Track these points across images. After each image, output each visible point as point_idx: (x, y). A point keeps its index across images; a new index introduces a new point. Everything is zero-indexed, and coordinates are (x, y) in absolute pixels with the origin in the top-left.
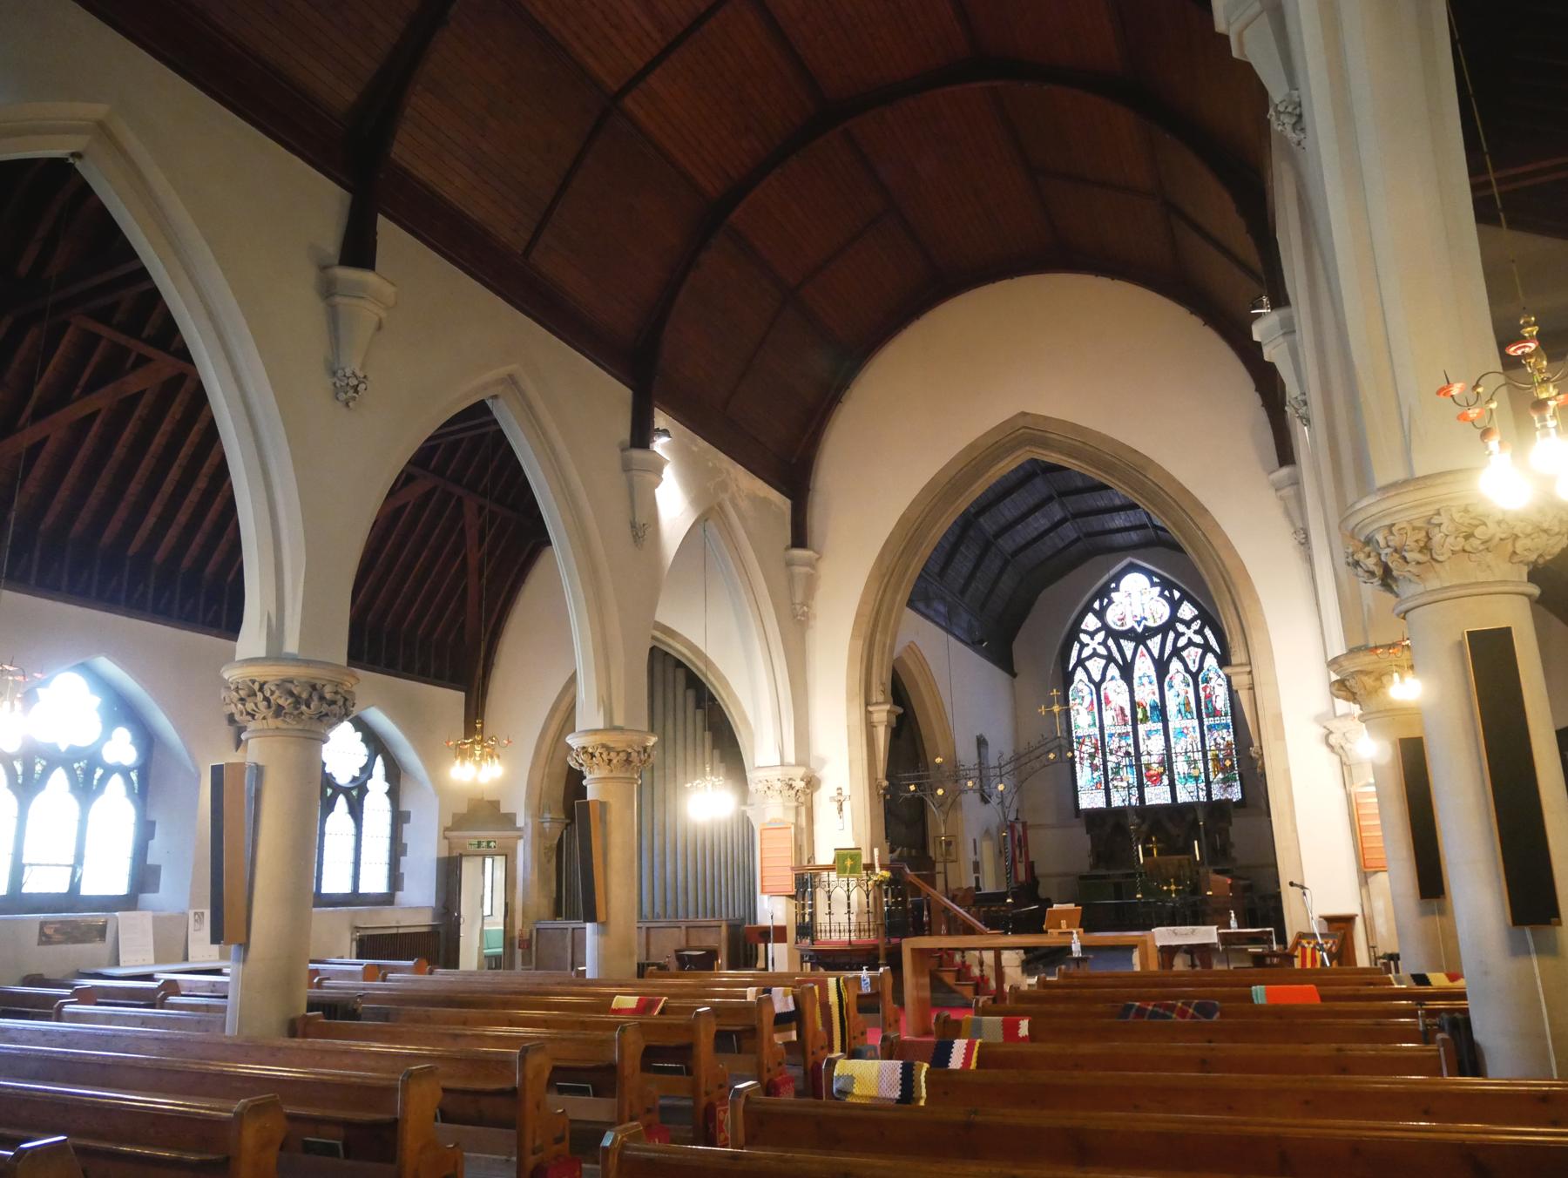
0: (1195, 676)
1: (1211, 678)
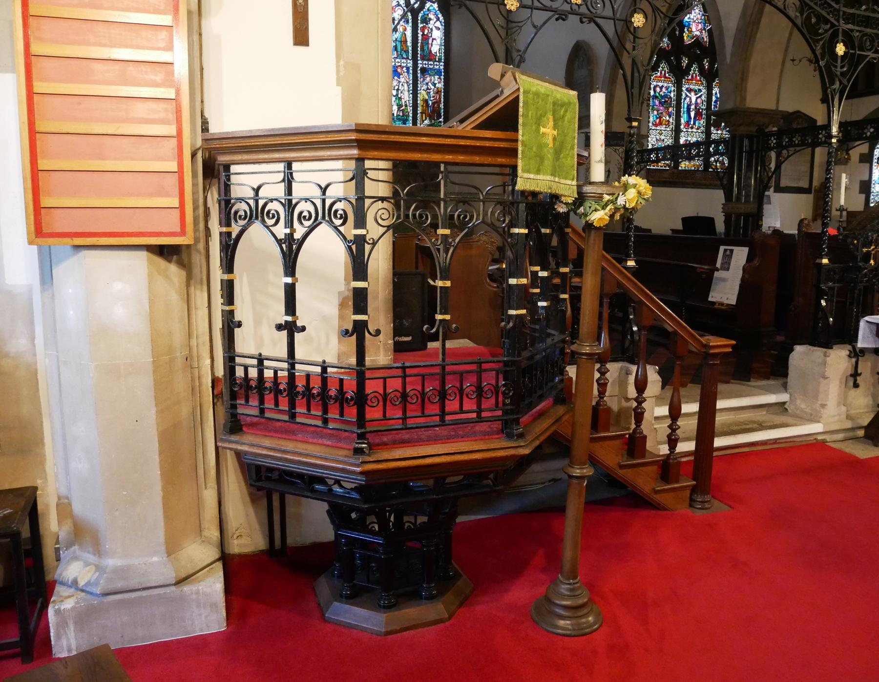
1: (430, 19)
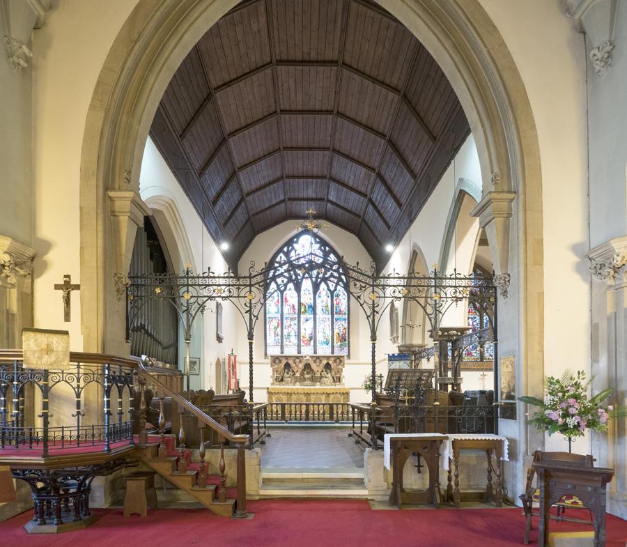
0: (332, 293)
